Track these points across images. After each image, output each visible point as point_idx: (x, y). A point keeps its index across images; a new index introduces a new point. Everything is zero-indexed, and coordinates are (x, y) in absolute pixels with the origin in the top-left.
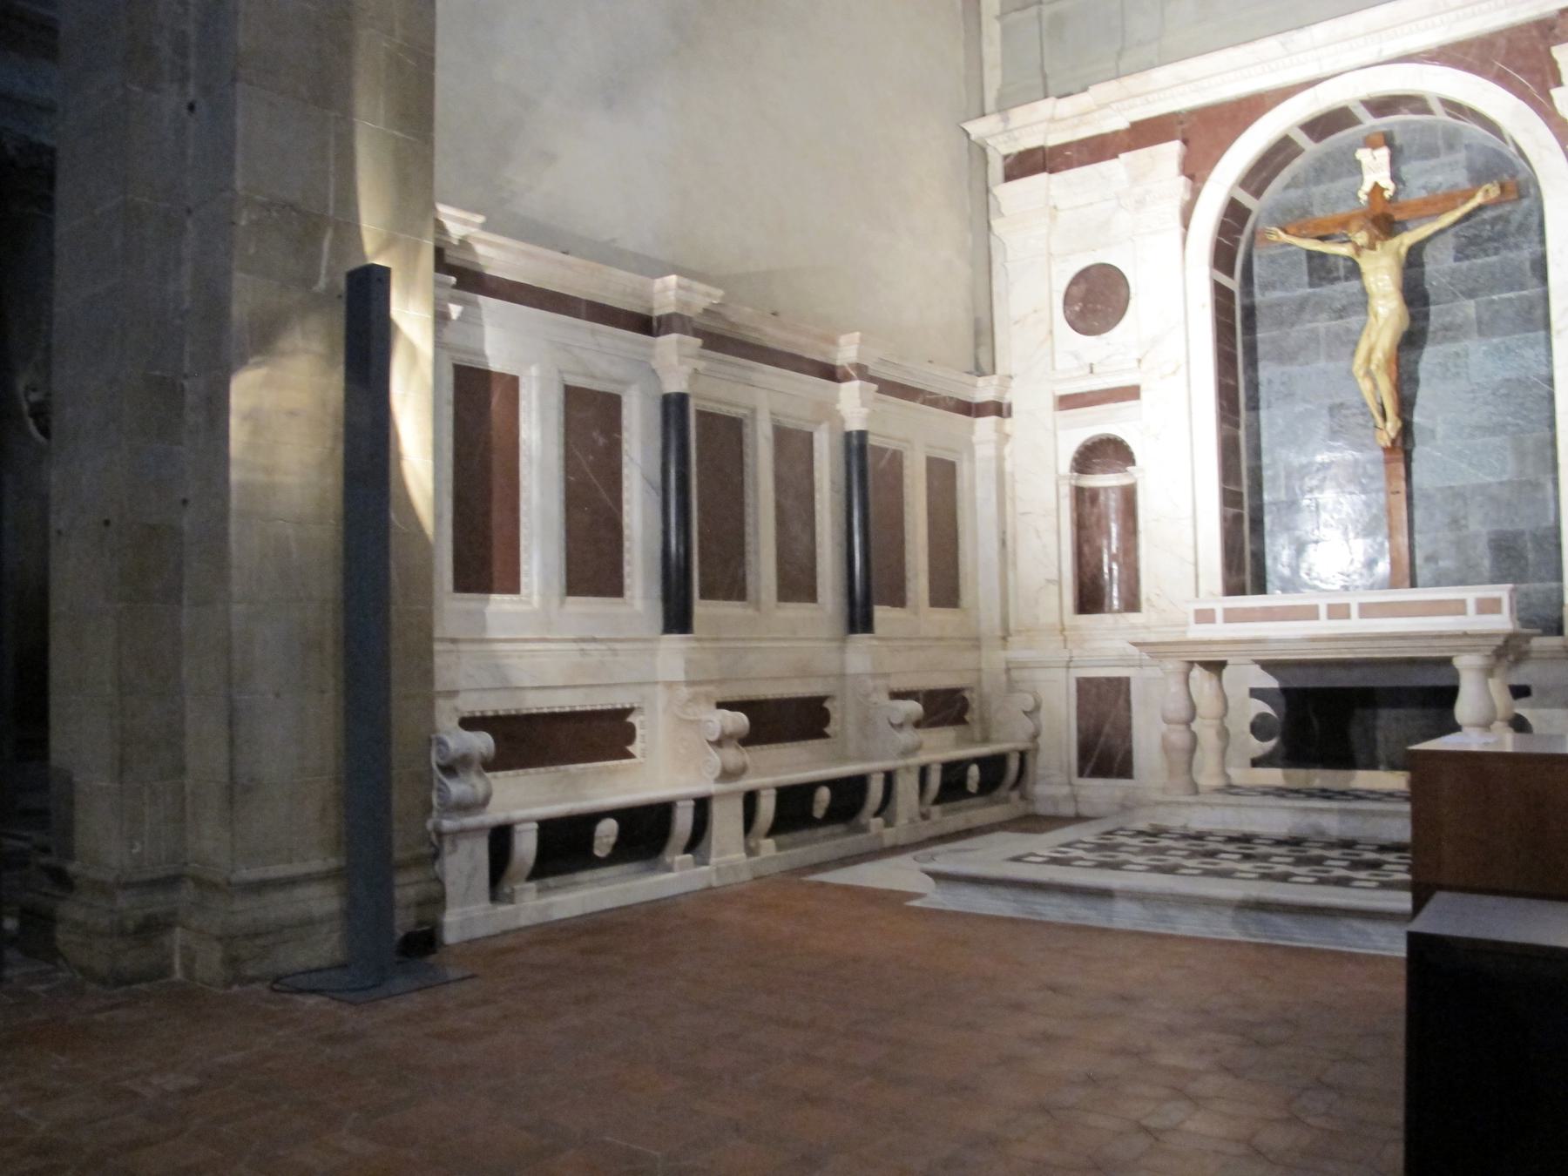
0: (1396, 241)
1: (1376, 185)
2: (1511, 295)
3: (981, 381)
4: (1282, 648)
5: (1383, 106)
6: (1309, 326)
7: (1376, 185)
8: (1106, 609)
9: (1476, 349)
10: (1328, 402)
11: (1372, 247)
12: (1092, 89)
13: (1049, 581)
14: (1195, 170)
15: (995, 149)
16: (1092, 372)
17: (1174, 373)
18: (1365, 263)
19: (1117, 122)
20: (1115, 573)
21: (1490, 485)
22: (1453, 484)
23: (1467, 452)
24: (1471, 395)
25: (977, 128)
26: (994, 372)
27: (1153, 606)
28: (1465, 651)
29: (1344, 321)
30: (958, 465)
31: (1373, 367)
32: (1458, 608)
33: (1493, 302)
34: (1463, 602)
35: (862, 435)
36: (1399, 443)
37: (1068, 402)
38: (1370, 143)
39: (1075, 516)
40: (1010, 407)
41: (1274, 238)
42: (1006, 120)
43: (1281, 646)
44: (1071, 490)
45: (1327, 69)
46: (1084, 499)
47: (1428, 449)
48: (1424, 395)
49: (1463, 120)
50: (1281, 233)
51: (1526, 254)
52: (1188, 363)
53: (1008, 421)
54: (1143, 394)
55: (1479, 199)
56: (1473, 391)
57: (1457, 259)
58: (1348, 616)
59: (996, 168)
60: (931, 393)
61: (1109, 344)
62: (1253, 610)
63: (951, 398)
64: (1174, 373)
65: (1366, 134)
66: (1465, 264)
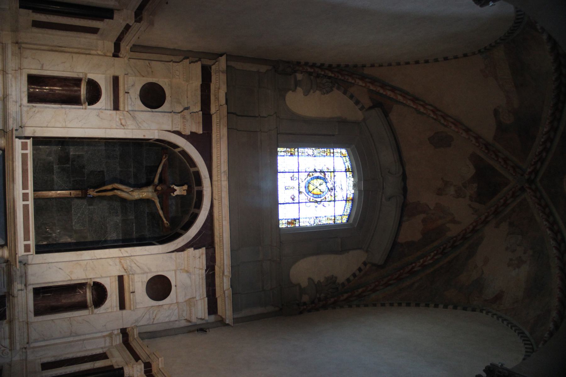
0: (156, 198)
1: (176, 190)
2: (134, 229)
3: (128, 48)
4: (11, 188)
5: (200, 195)
6: (132, 165)
7: (176, 190)
8: (29, 86)
9: (118, 219)
10: (105, 170)
11: (156, 190)
12: (225, 106)
13: (43, 65)
14: (192, 138)
15: (214, 64)
16: (126, 93)
17: (121, 124)
18: (150, 189)
19: (213, 110)
20: (45, 91)
21: (72, 223)
22: (73, 211)
23: (84, 216)
24: (103, 217)
25: (223, 59)
26: (131, 51)
27: (30, 109)
28: (10, 253)
29: (133, 177)
30: (96, 35)
31: (116, 191)
32: (27, 238)
33: (133, 224)
34: (29, 240)
35: (111, 18)
36: (88, 196)
37: (116, 80)
38: (189, 191)
39: (70, 78)
40: (118, 56)
41: (164, 157)
42: (223, 72)
43: (11, 187)
44: (81, 78)
45: (214, 183)
46: (77, 82)
47: (86, 204)
48: (105, 202)
49: (190, 217)
50: (165, 159)
51: (147, 234)
52: (125, 129)
53: (111, 55)
54: (114, 112)
55: (165, 221)
56: (104, 218)
57: (147, 212)
58: (23, 200)
59: (207, 62)
60: (126, 33)
61: (136, 99)
62: (27, 165)
63: (123, 37)
64: (121, 124)
65: (192, 186)
66: (146, 215)
